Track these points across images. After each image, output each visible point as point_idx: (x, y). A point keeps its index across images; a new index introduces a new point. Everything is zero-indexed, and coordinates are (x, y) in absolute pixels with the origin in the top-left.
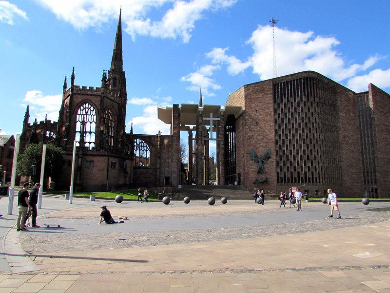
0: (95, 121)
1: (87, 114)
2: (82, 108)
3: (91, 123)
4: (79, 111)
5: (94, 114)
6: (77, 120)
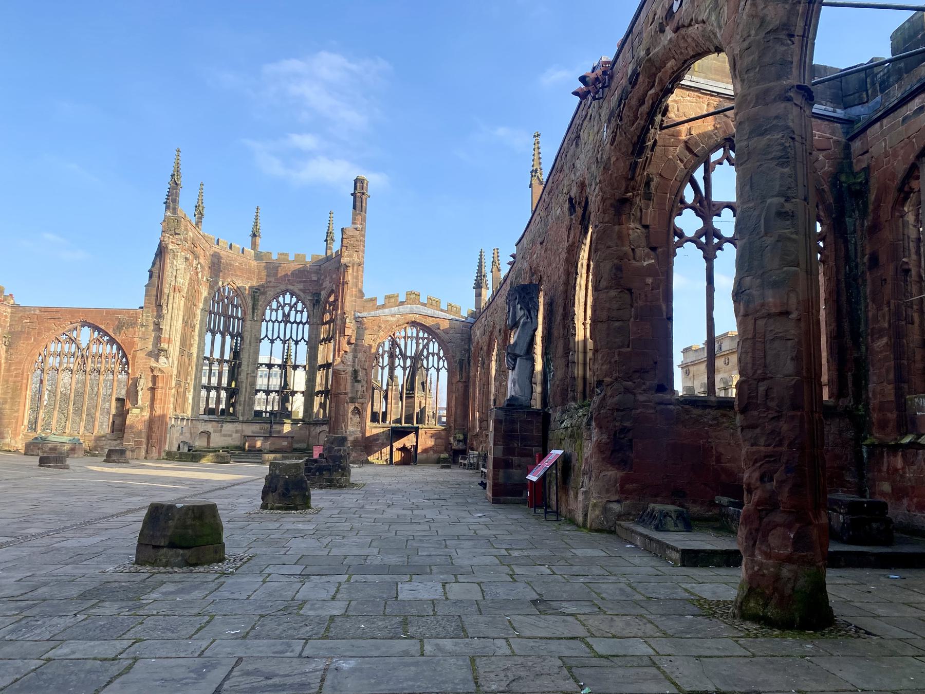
0: (306, 338)
1: (286, 319)
2: (274, 305)
4: (268, 312)
6: (263, 335)
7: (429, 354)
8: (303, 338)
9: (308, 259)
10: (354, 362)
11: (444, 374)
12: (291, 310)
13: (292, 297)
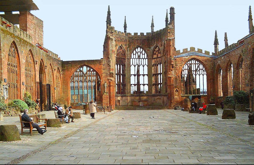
0: (147, 64)
3: (143, 66)
4: (132, 55)
5: (146, 58)
6: (131, 64)
7: (199, 69)
9: (145, 34)
10: (175, 73)
11: (205, 77)
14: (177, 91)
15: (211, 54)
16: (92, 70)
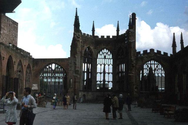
0: (112, 64)
1: (105, 58)
2: (101, 53)
3: (109, 65)
4: (99, 55)
5: (111, 58)
6: (98, 63)
7: (158, 69)
8: (111, 64)
9: (111, 37)
12: (106, 54)
13: (106, 50)
14: (136, 88)
15: (169, 55)
16: (59, 67)
